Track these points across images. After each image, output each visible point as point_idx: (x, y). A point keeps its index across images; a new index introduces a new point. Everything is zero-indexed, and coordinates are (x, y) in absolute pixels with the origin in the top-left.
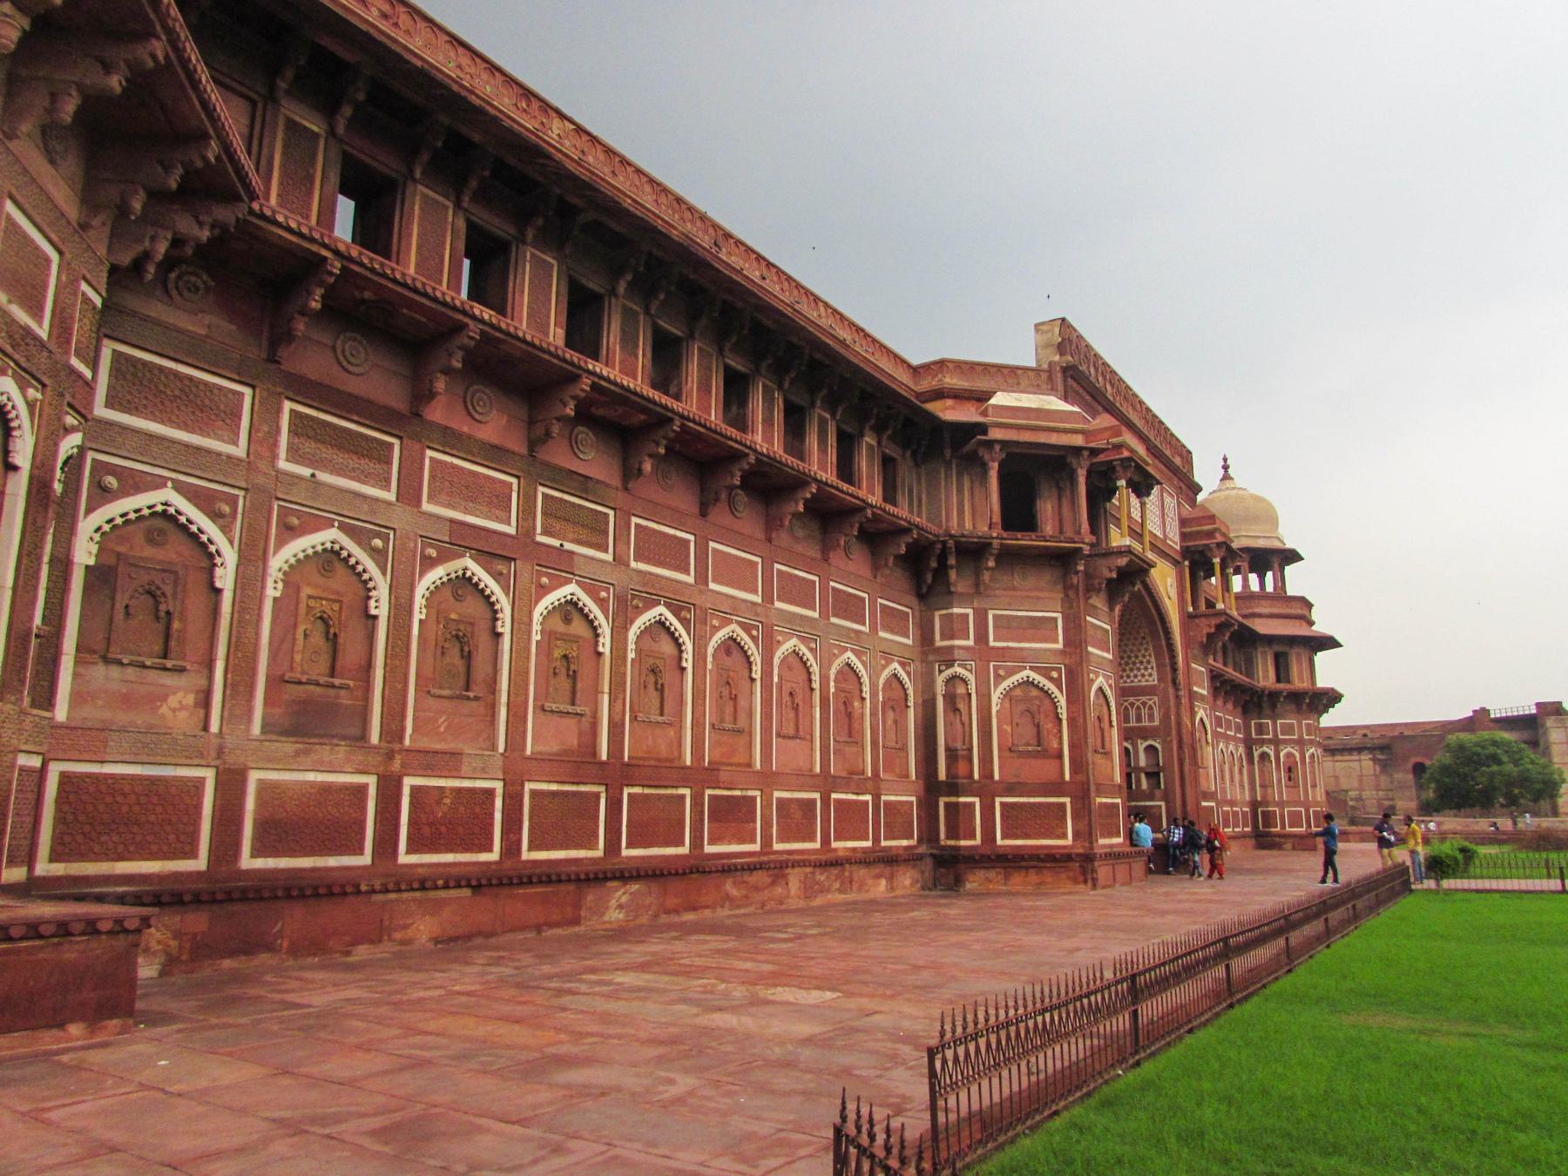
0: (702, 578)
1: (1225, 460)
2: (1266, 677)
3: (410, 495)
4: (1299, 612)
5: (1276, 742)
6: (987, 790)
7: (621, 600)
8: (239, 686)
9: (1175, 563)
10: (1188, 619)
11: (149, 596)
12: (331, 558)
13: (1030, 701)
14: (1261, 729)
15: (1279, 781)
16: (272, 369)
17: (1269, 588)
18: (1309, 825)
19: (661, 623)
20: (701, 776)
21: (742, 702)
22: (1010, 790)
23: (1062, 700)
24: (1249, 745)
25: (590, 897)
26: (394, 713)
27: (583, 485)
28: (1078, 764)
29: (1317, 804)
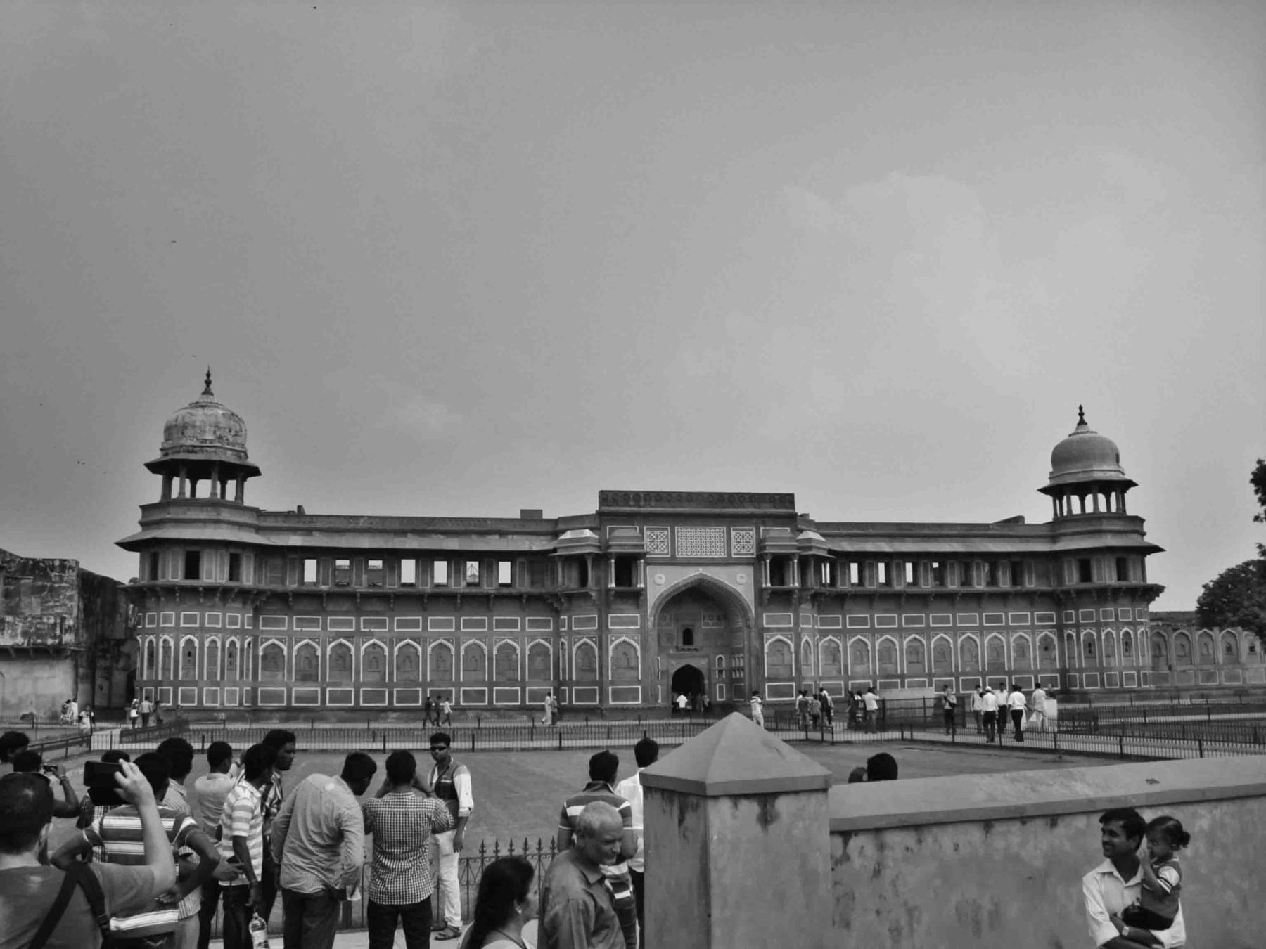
0: (425, 628)
1: (1081, 408)
2: (1071, 580)
3: (324, 628)
4: (1098, 528)
5: (1077, 626)
6: (570, 683)
7: (391, 641)
8: (290, 672)
9: (748, 564)
10: (759, 592)
11: (273, 659)
12: (307, 645)
13: (585, 649)
14: (1069, 617)
15: (1080, 654)
16: (289, 610)
17: (1114, 509)
18: (1102, 684)
19: (408, 644)
20: (424, 685)
21: (448, 663)
22: (577, 683)
23: (596, 649)
24: (1060, 629)
25: (382, 715)
26: (324, 674)
27: (377, 613)
28: (601, 675)
29: (1110, 669)
